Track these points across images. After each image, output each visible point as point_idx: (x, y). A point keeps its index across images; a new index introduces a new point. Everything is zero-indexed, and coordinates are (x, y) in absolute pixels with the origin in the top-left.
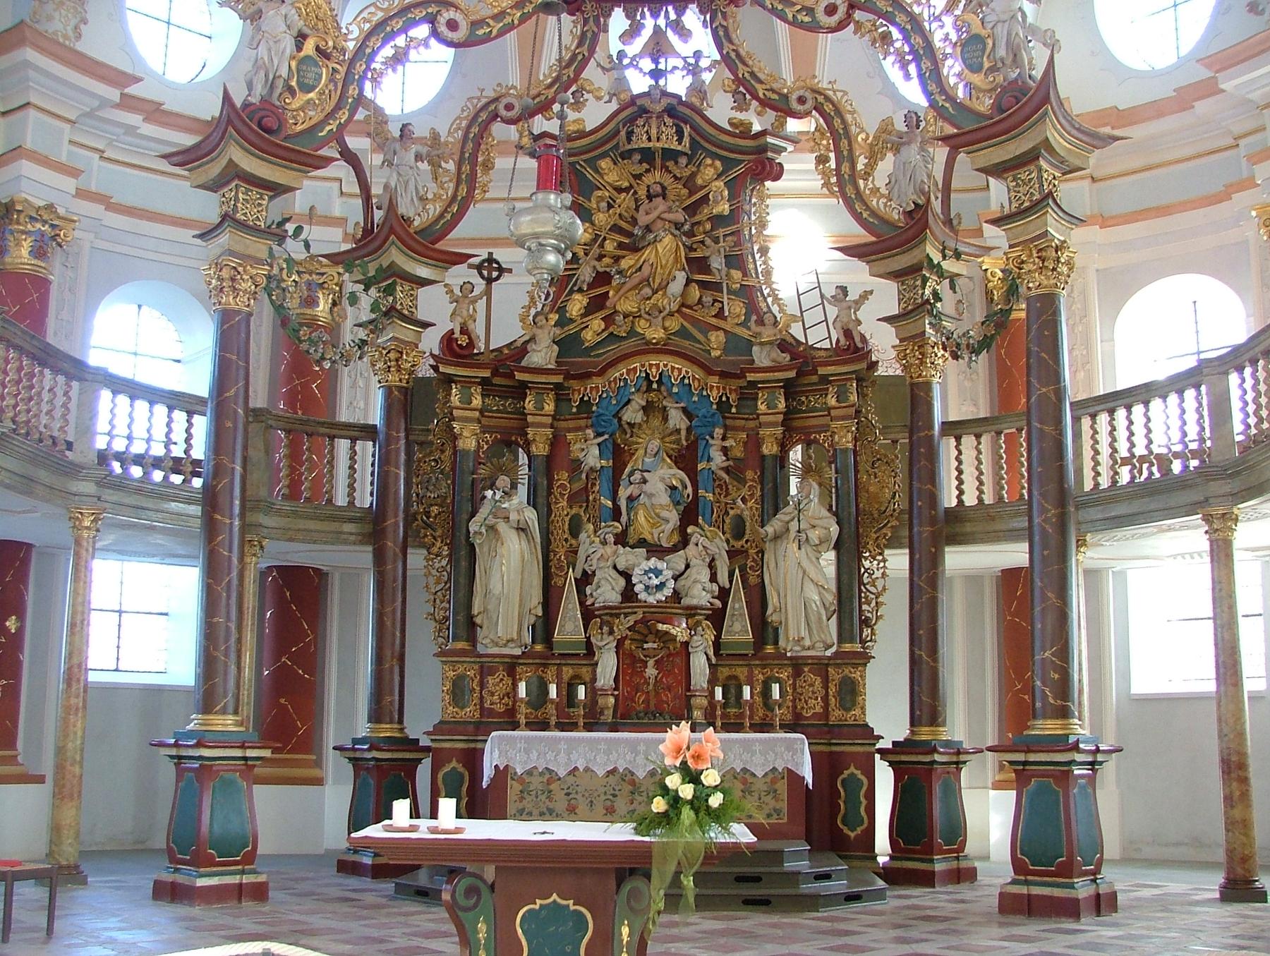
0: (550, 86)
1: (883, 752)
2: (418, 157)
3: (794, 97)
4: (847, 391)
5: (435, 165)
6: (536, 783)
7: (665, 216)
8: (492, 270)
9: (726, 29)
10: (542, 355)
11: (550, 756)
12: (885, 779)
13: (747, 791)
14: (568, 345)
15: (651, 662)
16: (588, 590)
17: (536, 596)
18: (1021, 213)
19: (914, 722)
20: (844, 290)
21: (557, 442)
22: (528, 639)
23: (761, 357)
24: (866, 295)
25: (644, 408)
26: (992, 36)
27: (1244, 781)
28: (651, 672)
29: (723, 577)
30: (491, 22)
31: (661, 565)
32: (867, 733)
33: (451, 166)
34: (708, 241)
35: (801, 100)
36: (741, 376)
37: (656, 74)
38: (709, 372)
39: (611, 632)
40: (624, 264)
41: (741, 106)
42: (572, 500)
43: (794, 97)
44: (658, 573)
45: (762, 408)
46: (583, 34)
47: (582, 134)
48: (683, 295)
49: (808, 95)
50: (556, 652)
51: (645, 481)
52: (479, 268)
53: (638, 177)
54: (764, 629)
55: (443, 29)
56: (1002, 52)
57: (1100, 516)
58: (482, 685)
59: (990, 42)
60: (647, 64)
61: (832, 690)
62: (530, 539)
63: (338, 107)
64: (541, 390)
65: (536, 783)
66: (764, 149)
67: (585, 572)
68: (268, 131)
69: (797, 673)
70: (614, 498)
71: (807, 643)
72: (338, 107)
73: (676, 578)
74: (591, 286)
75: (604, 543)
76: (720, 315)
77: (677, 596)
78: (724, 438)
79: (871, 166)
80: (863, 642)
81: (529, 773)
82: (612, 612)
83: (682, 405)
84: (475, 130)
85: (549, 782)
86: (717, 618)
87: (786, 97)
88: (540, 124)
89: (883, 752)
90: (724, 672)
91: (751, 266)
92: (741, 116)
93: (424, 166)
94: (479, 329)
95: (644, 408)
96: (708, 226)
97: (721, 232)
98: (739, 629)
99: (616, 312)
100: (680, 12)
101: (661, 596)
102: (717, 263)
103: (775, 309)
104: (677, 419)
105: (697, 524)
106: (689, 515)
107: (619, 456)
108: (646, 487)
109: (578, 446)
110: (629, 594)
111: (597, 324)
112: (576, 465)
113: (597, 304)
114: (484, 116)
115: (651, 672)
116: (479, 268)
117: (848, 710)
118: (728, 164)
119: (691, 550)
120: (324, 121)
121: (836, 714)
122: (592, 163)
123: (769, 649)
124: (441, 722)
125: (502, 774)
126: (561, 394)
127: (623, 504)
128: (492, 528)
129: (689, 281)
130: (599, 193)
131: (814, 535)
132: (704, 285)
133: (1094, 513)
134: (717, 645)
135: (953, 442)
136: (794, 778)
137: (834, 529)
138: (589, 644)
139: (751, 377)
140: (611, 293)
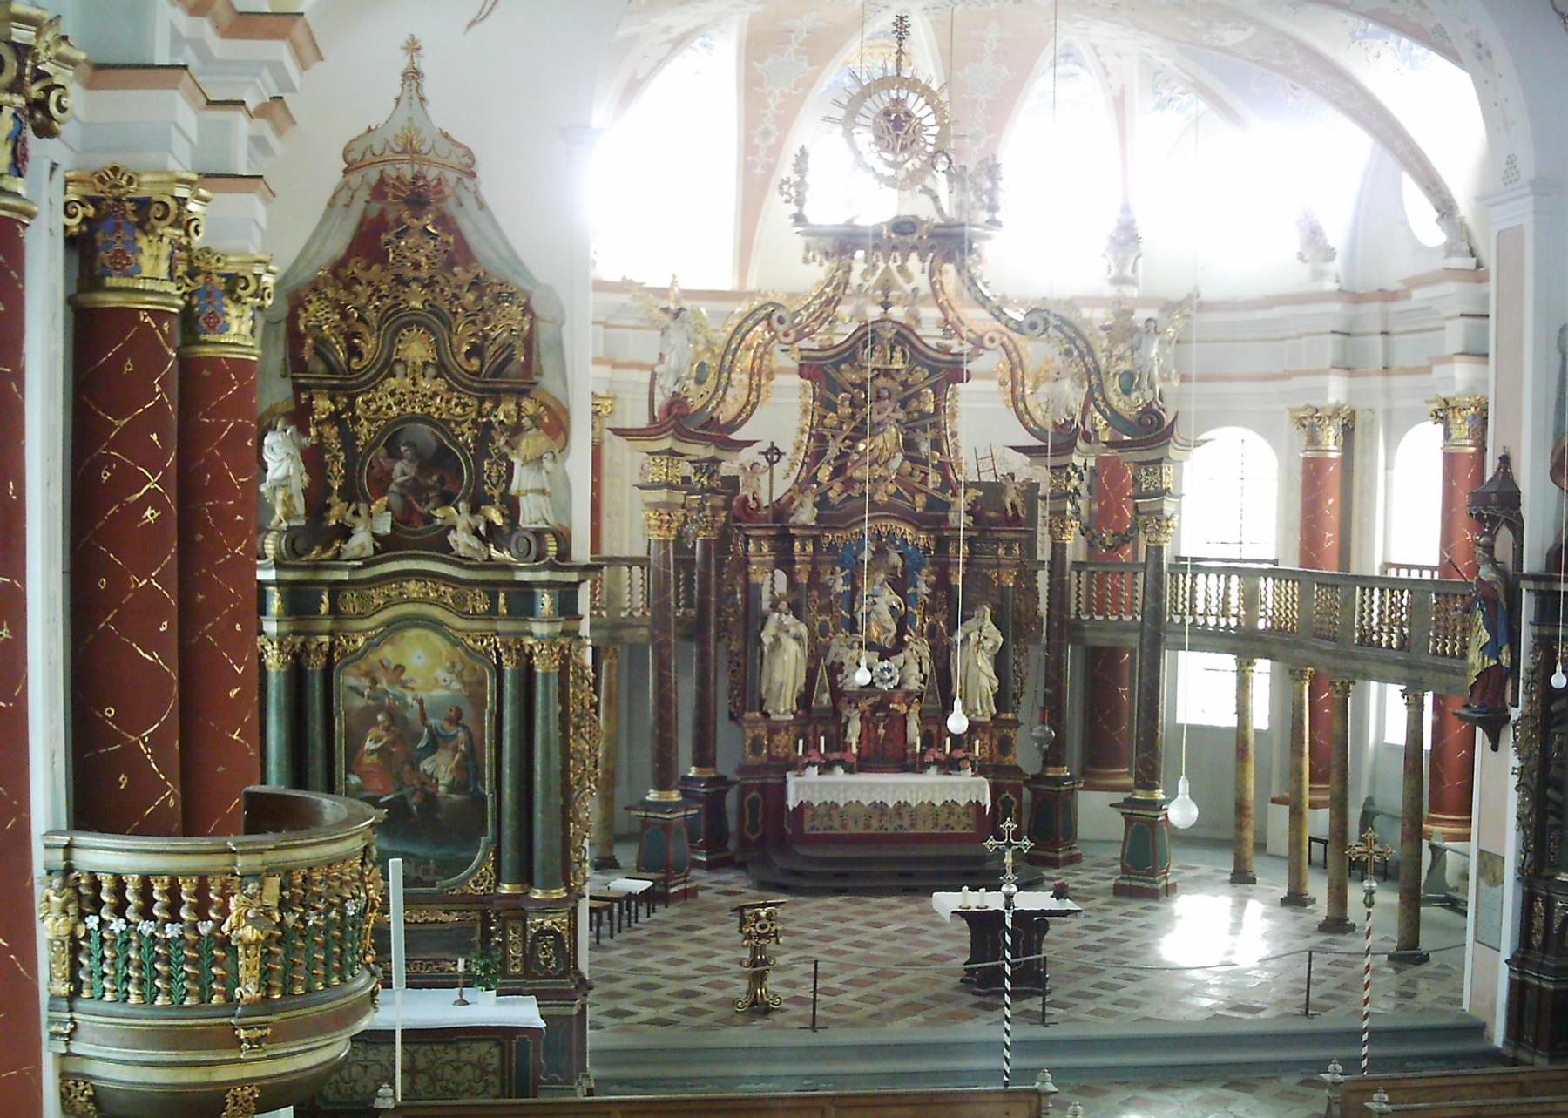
4: (1012, 548)
10: (806, 515)
11: (835, 793)
13: (951, 813)
14: (822, 503)
15: (882, 725)
16: (839, 678)
19: (1046, 763)
21: (814, 575)
22: (795, 708)
28: (881, 731)
30: (803, 312)
33: (745, 377)
37: (886, 305)
39: (856, 707)
43: (986, 338)
44: (889, 670)
47: (832, 347)
49: (997, 336)
50: (814, 715)
52: (765, 454)
61: (995, 742)
63: (716, 391)
70: (851, 610)
72: (716, 391)
74: (835, 460)
76: (924, 481)
79: (1035, 387)
85: (830, 810)
87: (981, 337)
88: (805, 343)
91: (945, 448)
96: (916, 415)
97: (928, 422)
100: (905, 258)
102: (925, 448)
104: (895, 559)
106: (903, 623)
107: (853, 580)
109: (828, 577)
111: (838, 486)
112: (826, 589)
113: (838, 471)
115: (881, 731)
116: (765, 454)
117: (1005, 755)
118: (933, 371)
119: (907, 653)
120: (710, 401)
122: (836, 366)
126: (816, 541)
128: (777, 639)
130: (843, 395)
132: (912, 460)
136: (978, 806)
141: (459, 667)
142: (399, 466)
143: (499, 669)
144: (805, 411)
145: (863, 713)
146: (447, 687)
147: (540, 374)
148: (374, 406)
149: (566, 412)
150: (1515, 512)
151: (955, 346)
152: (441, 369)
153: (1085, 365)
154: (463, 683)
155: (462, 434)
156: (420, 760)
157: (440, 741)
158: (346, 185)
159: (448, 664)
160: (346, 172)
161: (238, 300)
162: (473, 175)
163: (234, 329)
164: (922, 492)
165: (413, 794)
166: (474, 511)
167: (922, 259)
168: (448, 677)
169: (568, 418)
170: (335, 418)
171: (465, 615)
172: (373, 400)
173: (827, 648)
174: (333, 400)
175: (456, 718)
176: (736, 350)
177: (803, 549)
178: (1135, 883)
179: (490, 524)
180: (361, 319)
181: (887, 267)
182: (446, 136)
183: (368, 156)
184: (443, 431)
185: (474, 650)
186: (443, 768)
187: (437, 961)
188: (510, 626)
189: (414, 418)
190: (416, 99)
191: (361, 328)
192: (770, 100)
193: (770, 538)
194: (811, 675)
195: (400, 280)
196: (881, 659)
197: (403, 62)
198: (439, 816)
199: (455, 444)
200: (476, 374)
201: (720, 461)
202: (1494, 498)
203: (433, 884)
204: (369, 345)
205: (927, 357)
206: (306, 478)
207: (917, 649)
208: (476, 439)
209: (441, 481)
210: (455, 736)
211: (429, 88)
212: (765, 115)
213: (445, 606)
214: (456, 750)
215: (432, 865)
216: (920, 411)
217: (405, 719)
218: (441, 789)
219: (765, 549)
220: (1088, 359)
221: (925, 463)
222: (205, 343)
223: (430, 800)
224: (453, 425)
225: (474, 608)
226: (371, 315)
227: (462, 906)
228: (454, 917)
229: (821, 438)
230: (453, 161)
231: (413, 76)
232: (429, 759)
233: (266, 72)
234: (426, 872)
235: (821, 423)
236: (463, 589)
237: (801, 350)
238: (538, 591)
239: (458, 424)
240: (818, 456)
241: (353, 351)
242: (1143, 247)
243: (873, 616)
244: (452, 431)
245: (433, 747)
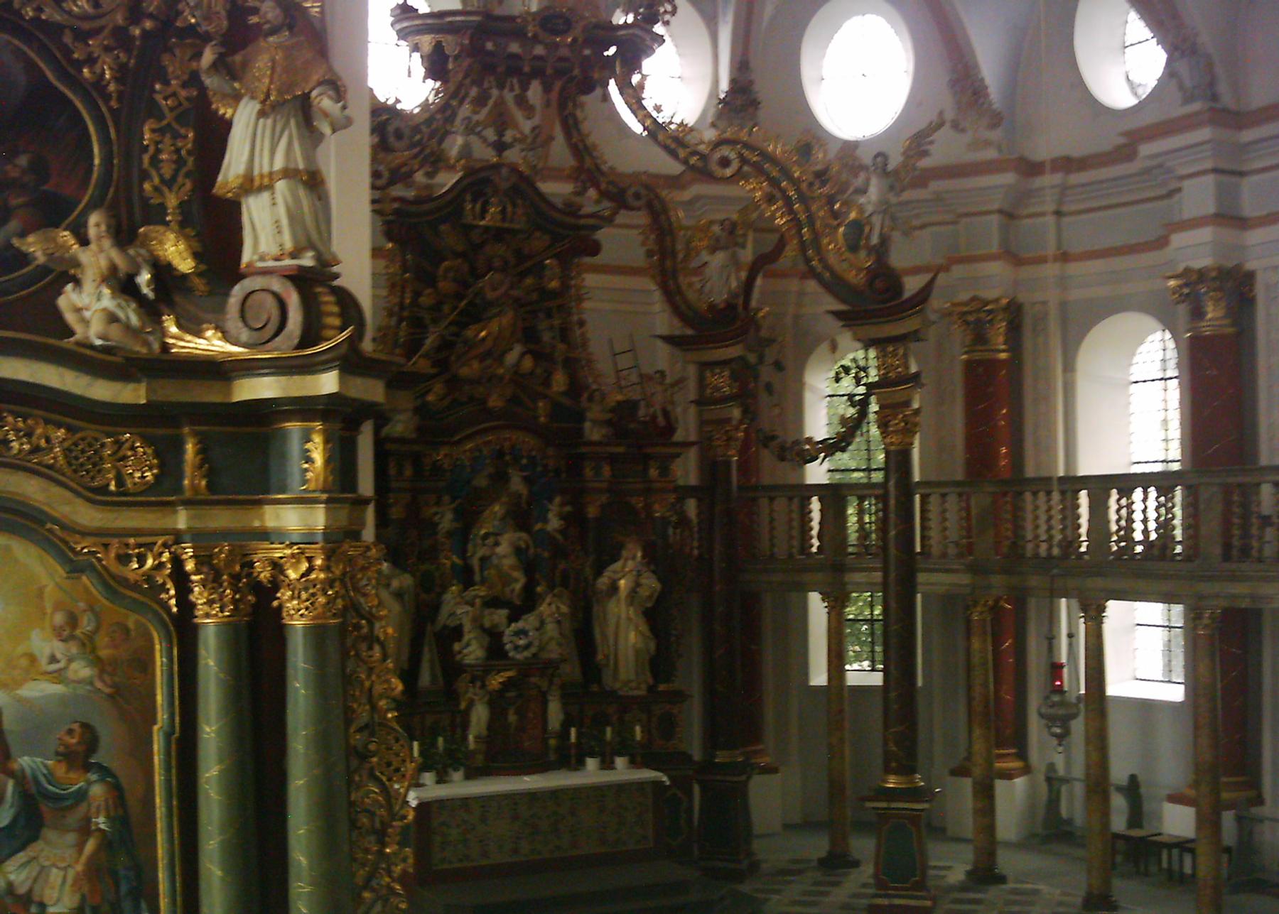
3: (631, 192)
7: (512, 292)
23: (593, 432)
26: (869, 223)
28: (512, 718)
34: (541, 315)
37: (500, 147)
39: (483, 686)
40: (469, 333)
43: (631, 192)
45: (589, 472)
47: (430, 199)
48: (518, 364)
49: (643, 192)
51: (497, 544)
55: (392, 139)
57: (864, 580)
59: (867, 229)
60: (490, 134)
70: (463, 553)
71: (634, 684)
74: (439, 349)
76: (547, 383)
78: (563, 504)
83: (525, 474)
87: (622, 192)
88: (398, 191)
92: (578, 199)
98: (571, 671)
100: (525, 88)
101: (526, 654)
104: (517, 484)
107: (468, 518)
108: (499, 550)
119: (543, 608)
127: (475, 563)
140: (453, 358)
141: (86, 624)
144: (393, 286)
146: (58, 677)
151: (591, 202)
154: (97, 662)
155: (91, 61)
157: (46, 808)
159: (59, 618)
164: (545, 397)
166: (124, 235)
167: (547, 89)
168: (58, 648)
171: (97, 496)
173: (436, 607)
178: (897, 902)
179: (163, 271)
181: (501, 97)
184: (43, 50)
185: (124, 582)
186: (55, 875)
188: (221, 519)
196: (513, 618)
199: (75, 83)
208: (122, 73)
209: (39, 169)
210: (82, 795)
213: (46, 473)
214: (85, 830)
224: (68, 39)
225: (120, 481)
229: (418, 325)
232: (21, 857)
235: (415, 302)
236: (90, 431)
238: (294, 427)
239: (82, 36)
242: (762, 114)
243: (495, 561)
244: (68, 52)
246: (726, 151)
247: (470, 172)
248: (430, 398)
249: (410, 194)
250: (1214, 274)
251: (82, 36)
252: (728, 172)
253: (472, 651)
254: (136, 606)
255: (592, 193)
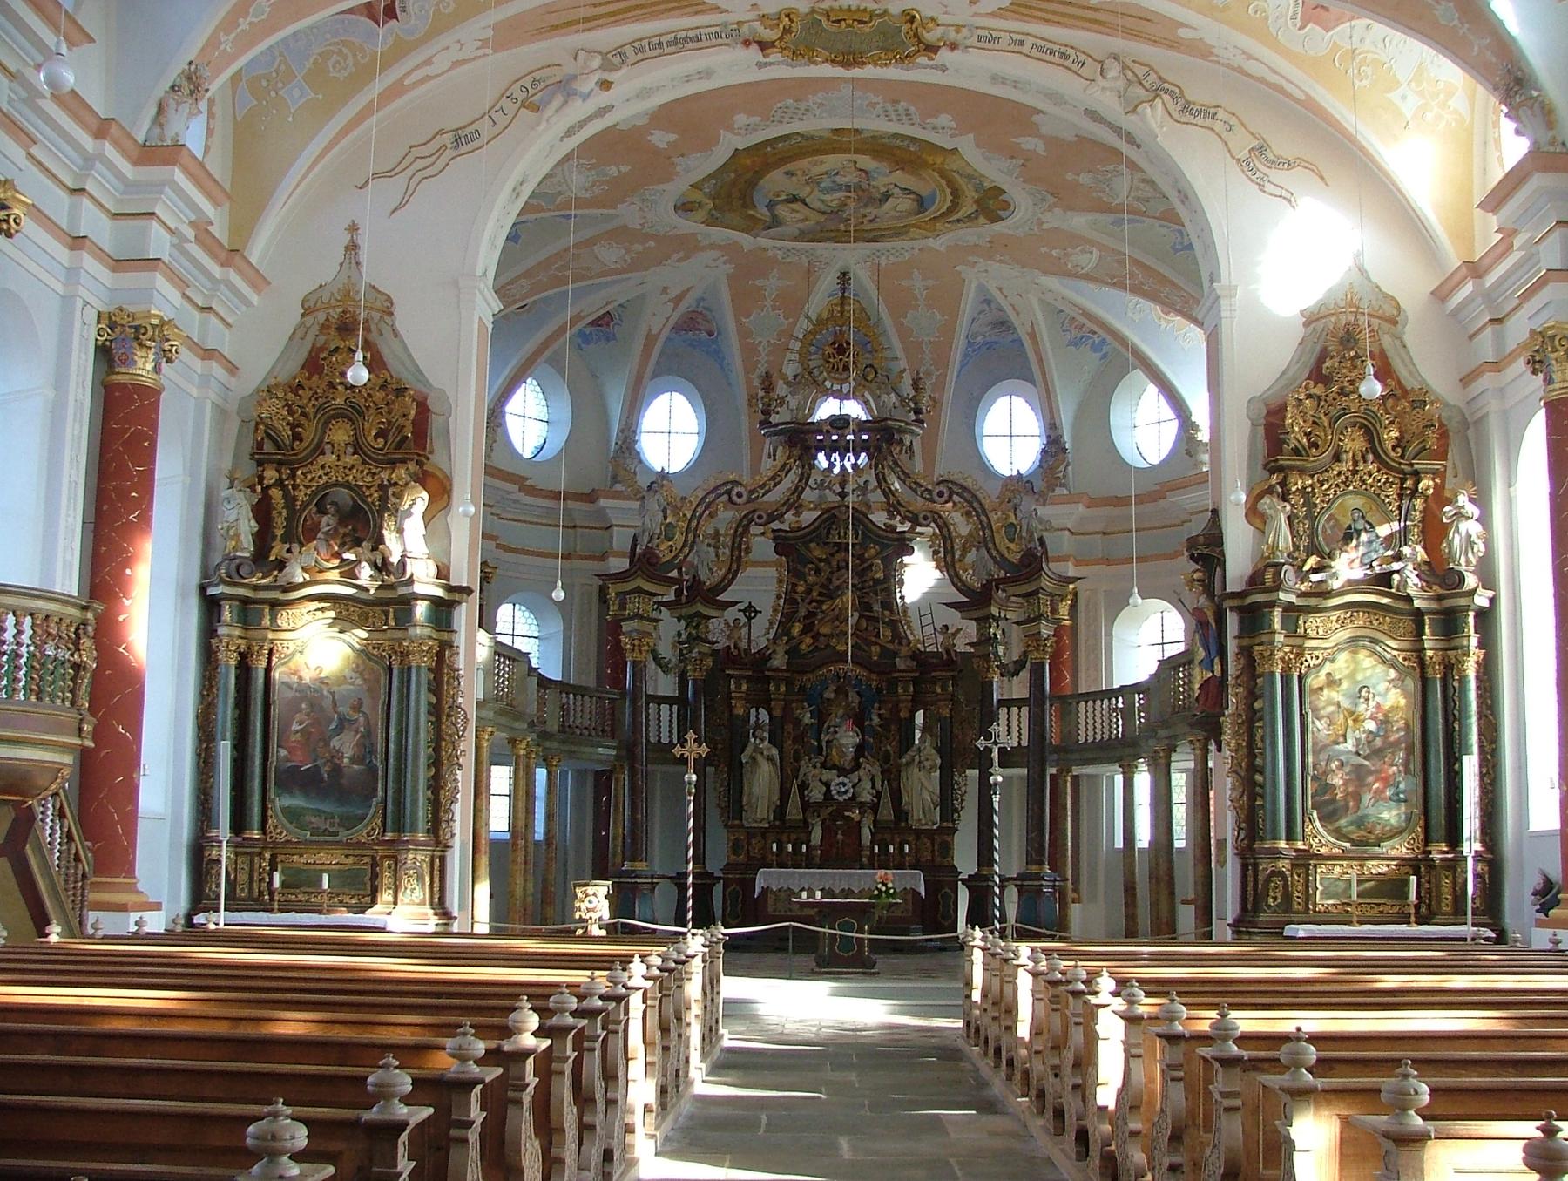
0: (783, 505)
1: (963, 881)
2: (709, 545)
5: (716, 548)
6: (782, 895)
8: (751, 612)
9: (884, 474)
10: (779, 661)
12: (963, 896)
14: (792, 652)
17: (776, 798)
18: (1028, 621)
20: (946, 627)
21: (787, 709)
23: (901, 664)
24: (959, 630)
25: (835, 691)
27: (1134, 895)
28: (840, 837)
29: (878, 786)
31: (846, 781)
32: (954, 871)
33: (727, 551)
35: (925, 518)
36: (890, 673)
38: (871, 671)
40: (824, 607)
41: (892, 517)
42: (795, 741)
44: (844, 785)
45: (900, 691)
46: (802, 474)
47: (800, 529)
51: (836, 732)
52: (744, 611)
53: (832, 555)
54: (901, 814)
55: (735, 498)
56: (1024, 534)
58: (749, 844)
62: (774, 764)
64: (778, 681)
65: (782, 895)
66: (905, 539)
67: (803, 782)
68: (650, 564)
69: (918, 838)
70: (819, 740)
73: (853, 787)
74: (805, 618)
75: (815, 767)
76: (878, 636)
77: (854, 797)
79: (963, 556)
80: (953, 821)
81: (780, 890)
82: (819, 805)
84: (740, 530)
86: (875, 807)
87: (917, 516)
88: (775, 525)
89: (963, 881)
90: (879, 837)
93: (711, 550)
94: (744, 645)
95: (835, 691)
97: (879, 588)
98: (886, 813)
99: (818, 634)
102: (877, 607)
103: (908, 632)
104: (853, 697)
105: (864, 756)
107: (821, 716)
108: (837, 736)
110: (828, 793)
111: (808, 640)
112: (798, 722)
114: (745, 522)
115: (840, 837)
116: (744, 611)
118: (884, 547)
119: (861, 772)
121: (938, 859)
123: (903, 824)
124: (727, 864)
125: (765, 891)
126: (789, 683)
127: (824, 744)
128: (754, 759)
129: (861, 616)
131: (927, 764)
132: (869, 619)
133: (1076, 756)
134: (875, 822)
135: (1005, 709)
137: (939, 761)
138: (805, 822)
139: (895, 675)
142: (325, 519)
143: (390, 669)
144: (780, 581)
145: (823, 822)
146: (352, 684)
147: (431, 452)
148: (309, 477)
149: (450, 480)
150: (1218, 550)
152: (357, 448)
153: (981, 522)
156: (330, 738)
157: (346, 724)
158: (302, 324)
160: (303, 315)
161: (141, 345)
162: (391, 314)
163: (140, 362)
164: (876, 644)
165: (325, 764)
169: (451, 485)
170: (280, 483)
172: (310, 472)
174: (278, 471)
175: (357, 707)
176: (701, 515)
177: (777, 689)
180: (303, 414)
182: (374, 287)
183: (319, 304)
184: (358, 495)
187: (338, 895)
189: (337, 484)
190: (354, 265)
191: (303, 420)
192: (761, 349)
193: (749, 679)
194: (784, 794)
195: (332, 386)
197: (346, 239)
198: (344, 781)
200: (381, 450)
201: (709, 618)
202: (1201, 539)
203: (336, 834)
204: (310, 432)
205: (879, 536)
206: (253, 523)
207: (870, 768)
211: (364, 256)
212: (759, 361)
214: (357, 732)
215: (337, 820)
216: (873, 579)
217: (321, 707)
218: (346, 760)
219: (744, 687)
220: (983, 518)
221: (875, 620)
222: (119, 373)
223: (337, 770)
226: (310, 410)
227: (357, 852)
228: (350, 860)
229: (790, 601)
230: (378, 305)
231: (352, 248)
233: (167, 189)
234: (332, 825)
236: (367, 609)
237: (773, 531)
239: (368, 488)
240: (787, 620)
241: (297, 437)
245: (340, 728)
246: (941, 487)
247: (826, 511)
248: (803, 647)
249: (785, 527)
250: (1201, 539)
251: (368, 488)
252: (943, 499)
253: (817, 794)
254: (377, 663)
255: (898, 518)
